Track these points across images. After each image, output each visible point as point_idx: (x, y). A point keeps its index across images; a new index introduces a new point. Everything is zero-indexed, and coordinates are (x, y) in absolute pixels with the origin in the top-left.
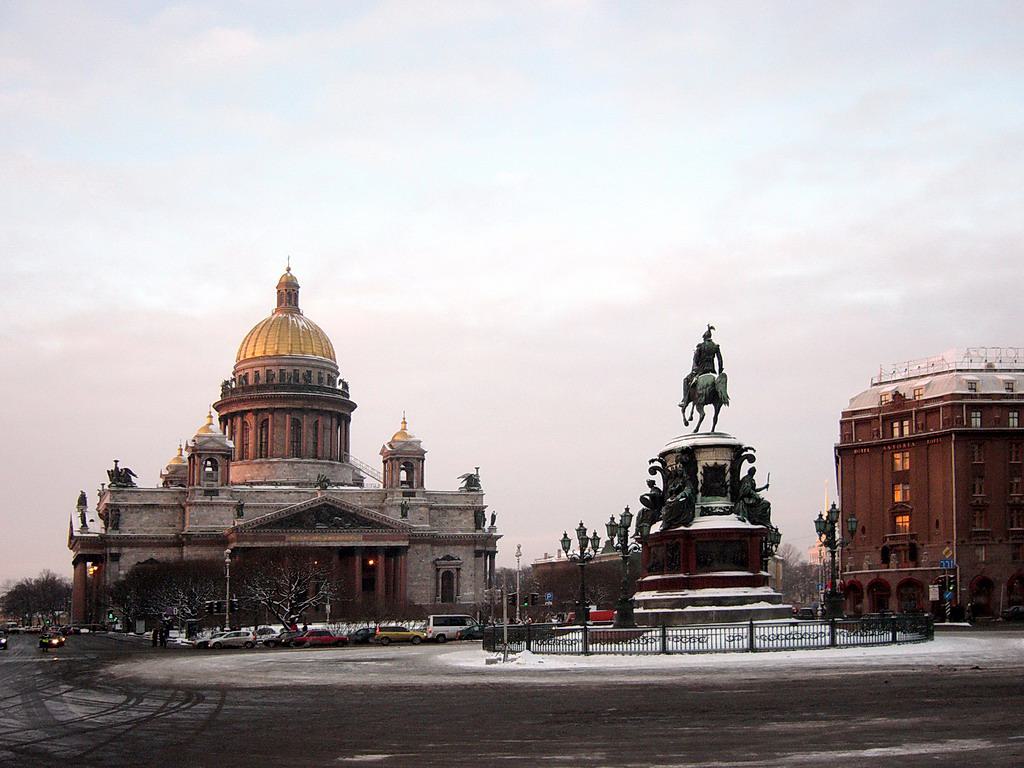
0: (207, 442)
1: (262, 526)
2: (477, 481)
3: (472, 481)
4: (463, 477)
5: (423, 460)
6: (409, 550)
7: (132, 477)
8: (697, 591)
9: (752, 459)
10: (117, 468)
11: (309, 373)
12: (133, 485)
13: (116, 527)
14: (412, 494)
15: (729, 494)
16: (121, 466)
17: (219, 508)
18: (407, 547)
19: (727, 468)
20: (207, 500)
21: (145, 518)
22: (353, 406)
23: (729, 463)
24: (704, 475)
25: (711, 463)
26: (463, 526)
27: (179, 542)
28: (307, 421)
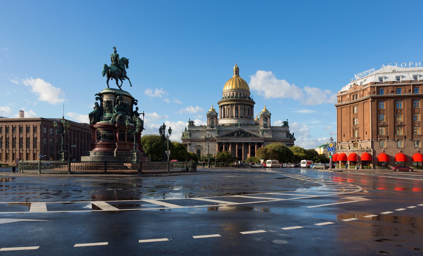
3: (286, 124)
10: (190, 121)
12: (194, 125)
14: (267, 127)
16: (191, 120)
17: (214, 131)
18: (263, 143)
21: (197, 134)
22: (254, 103)
26: (283, 135)
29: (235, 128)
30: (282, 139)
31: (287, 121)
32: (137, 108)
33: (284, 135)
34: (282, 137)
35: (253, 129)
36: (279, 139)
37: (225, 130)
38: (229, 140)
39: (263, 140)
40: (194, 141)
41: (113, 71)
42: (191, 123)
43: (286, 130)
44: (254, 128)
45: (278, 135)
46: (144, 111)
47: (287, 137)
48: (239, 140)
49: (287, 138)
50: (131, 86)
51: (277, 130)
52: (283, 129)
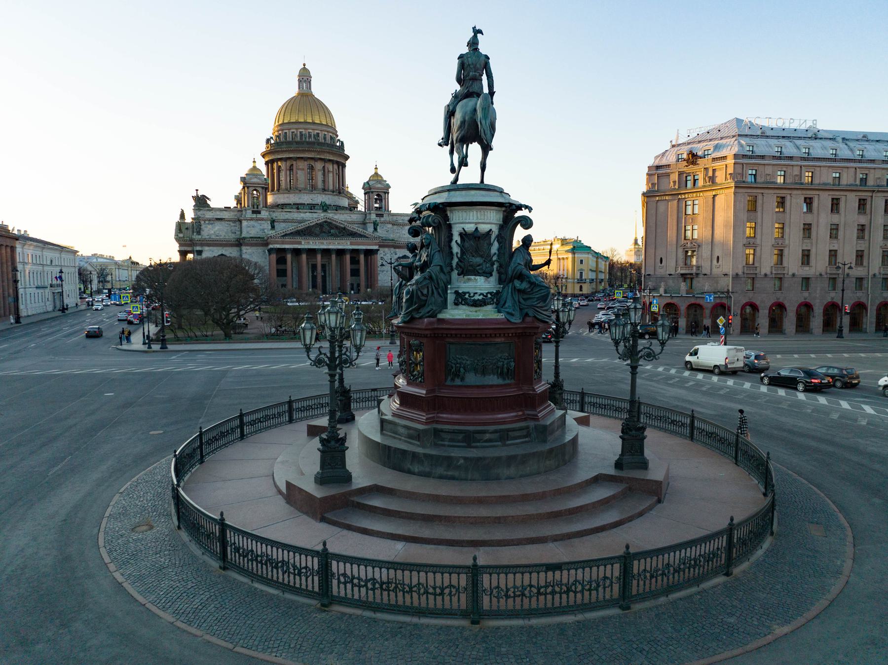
0: (251, 179)
1: (286, 235)
5: (388, 193)
7: (208, 201)
9: (527, 223)
11: (318, 134)
12: (208, 206)
13: (199, 233)
14: (381, 216)
15: (495, 273)
16: (200, 194)
17: (259, 222)
18: (378, 250)
19: (493, 237)
20: (254, 216)
22: (347, 158)
24: (461, 246)
25: (470, 228)
27: (239, 243)
28: (319, 166)
29: (311, 214)
35: (349, 218)
37: (286, 218)
38: (300, 243)
39: (376, 245)
40: (209, 245)
42: (201, 202)
44: (352, 216)
48: (322, 243)
51: (401, 222)
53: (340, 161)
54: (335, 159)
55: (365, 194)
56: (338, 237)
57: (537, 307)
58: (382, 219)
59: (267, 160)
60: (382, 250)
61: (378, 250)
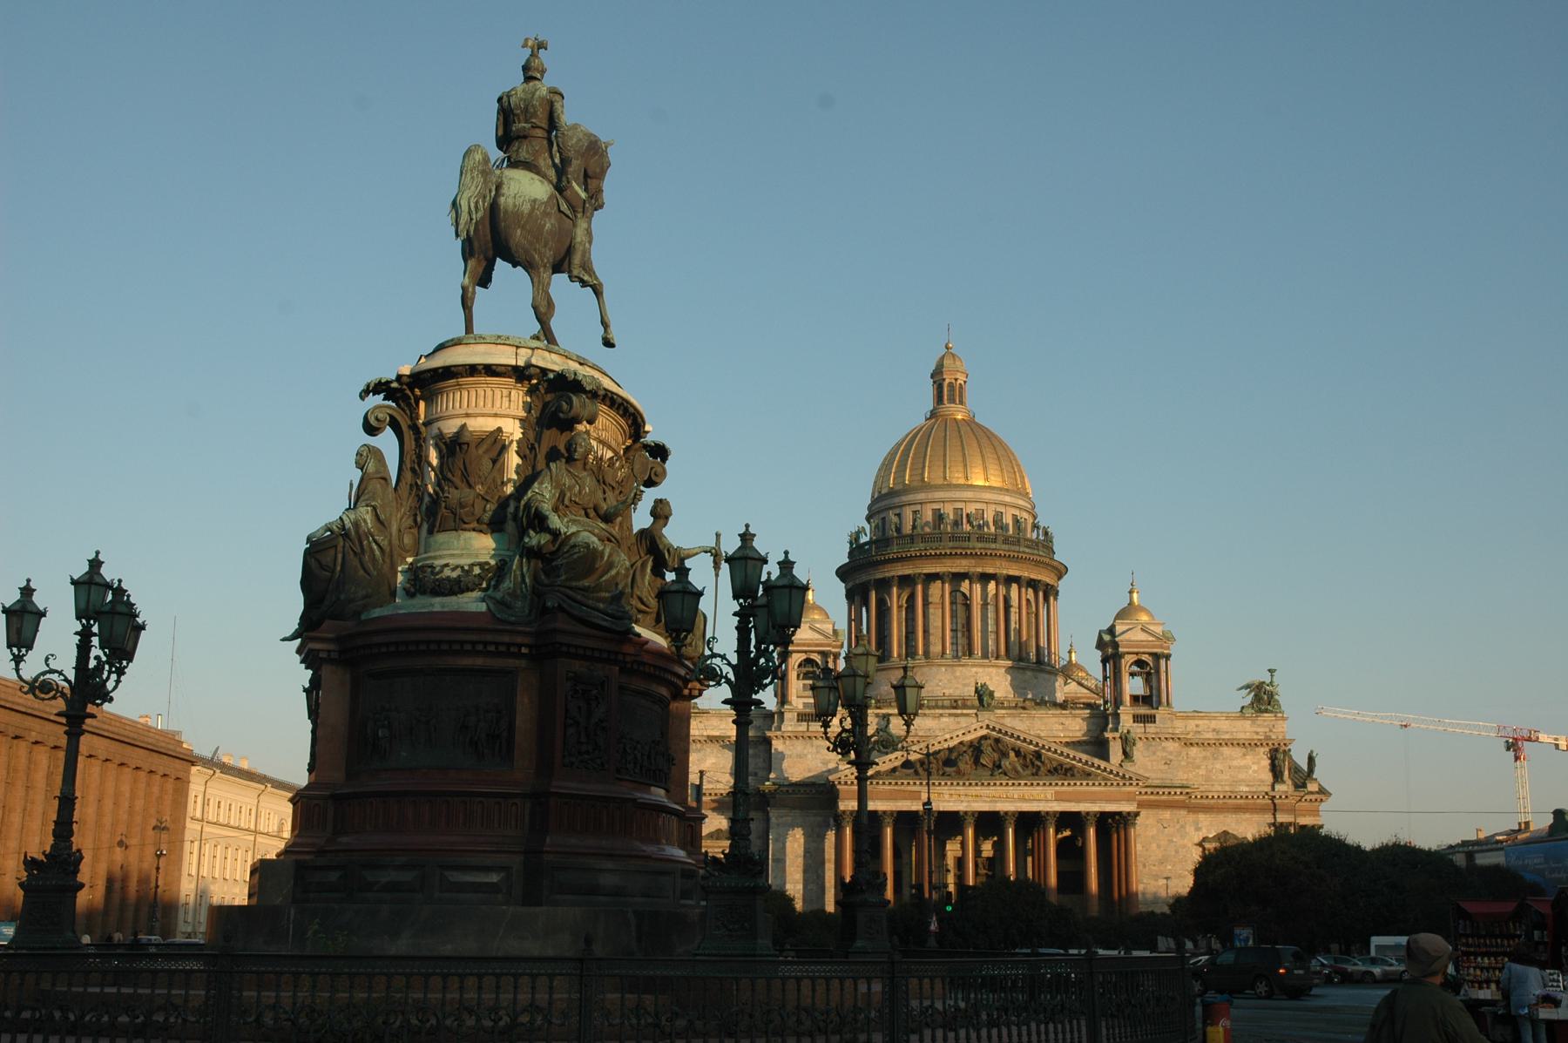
2: (1271, 695)
3: (1262, 698)
4: (1247, 687)
5: (1168, 657)
6: (1139, 820)
8: (827, 857)
14: (1150, 719)
22: (1061, 571)
23: (513, 430)
25: (450, 427)
29: (952, 719)
30: (1245, 789)
31: (1268, 681)
32: (661, 512)
33: (1255, 767)
34: (1242, 776)
35: (1061, 727)
36: (1227, 788)
41: (526, 208)
43: (1268, 738)
44: (1068, 722)
45: (1218, 766)
46: (718, 536)
47: (1277, 774)
49: (1278, 787)
50: (608, 343)
52: (1246, 729)
53: (1039, 577)
54: (1026, 574)
55: (1104, 661)
56: (1018, 776)
57: (571, 588)
58: (1151, 728)
59: (850, 584)
60: (1143, 813)
61: (1137, 814)
